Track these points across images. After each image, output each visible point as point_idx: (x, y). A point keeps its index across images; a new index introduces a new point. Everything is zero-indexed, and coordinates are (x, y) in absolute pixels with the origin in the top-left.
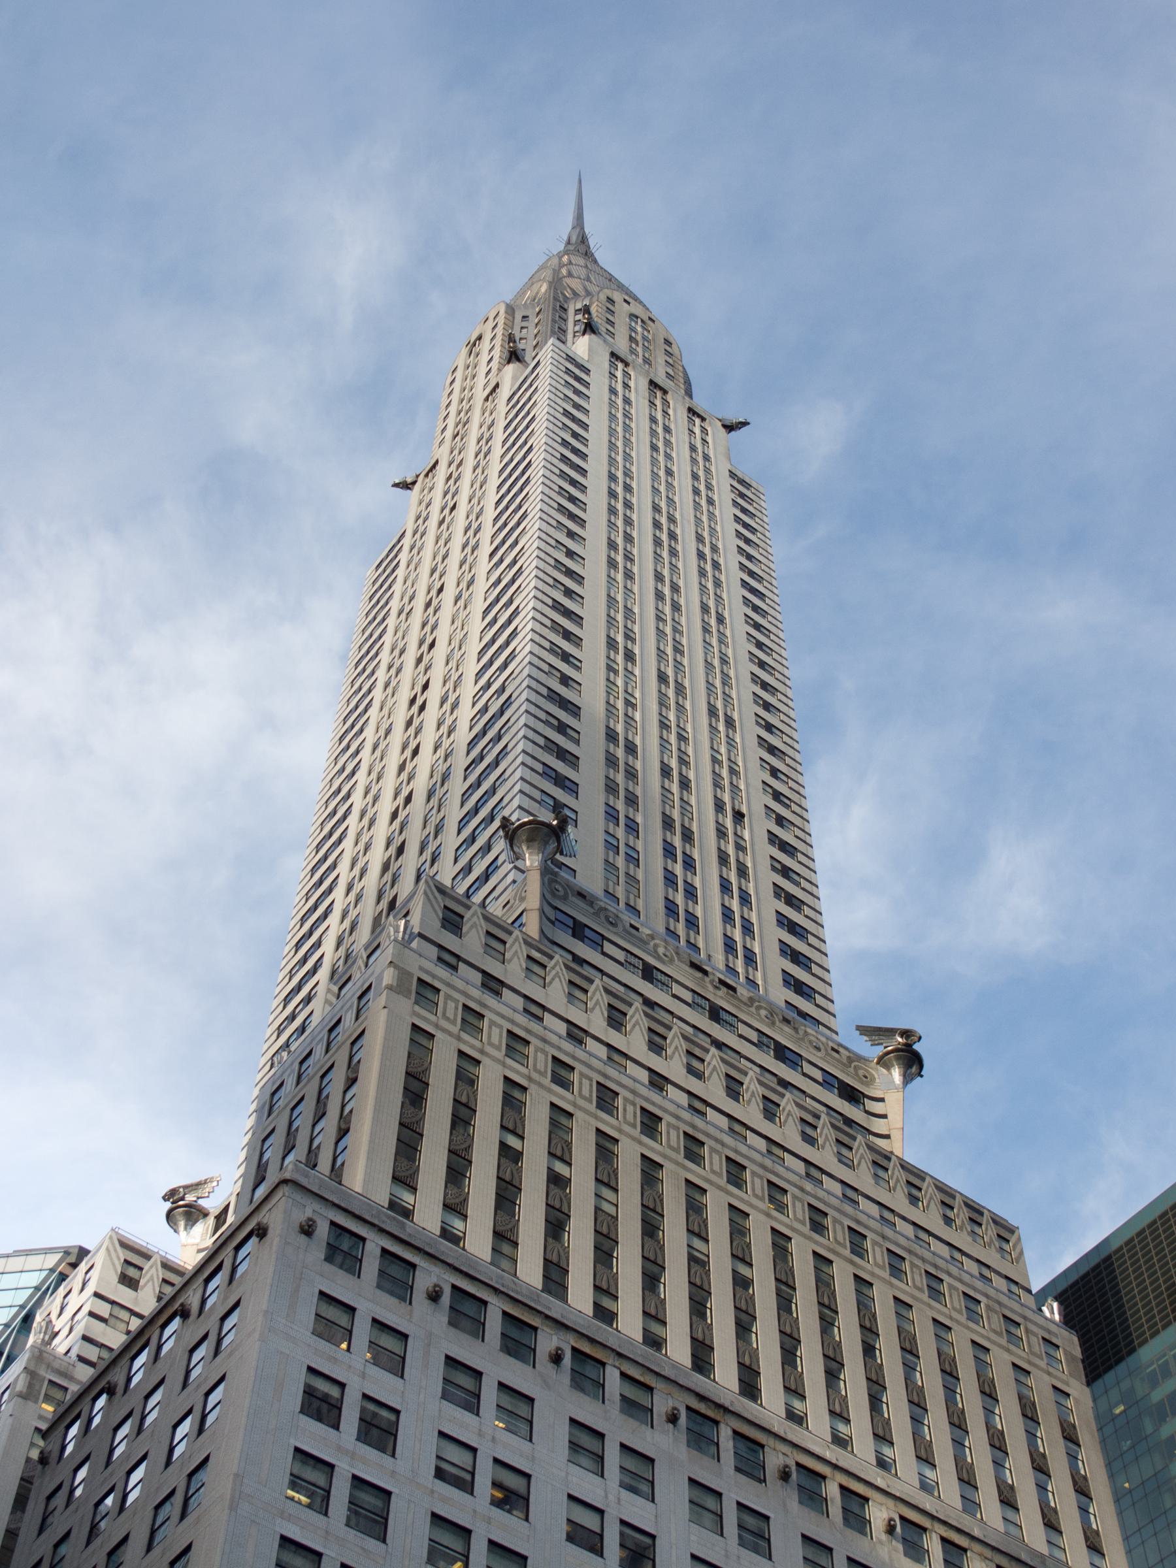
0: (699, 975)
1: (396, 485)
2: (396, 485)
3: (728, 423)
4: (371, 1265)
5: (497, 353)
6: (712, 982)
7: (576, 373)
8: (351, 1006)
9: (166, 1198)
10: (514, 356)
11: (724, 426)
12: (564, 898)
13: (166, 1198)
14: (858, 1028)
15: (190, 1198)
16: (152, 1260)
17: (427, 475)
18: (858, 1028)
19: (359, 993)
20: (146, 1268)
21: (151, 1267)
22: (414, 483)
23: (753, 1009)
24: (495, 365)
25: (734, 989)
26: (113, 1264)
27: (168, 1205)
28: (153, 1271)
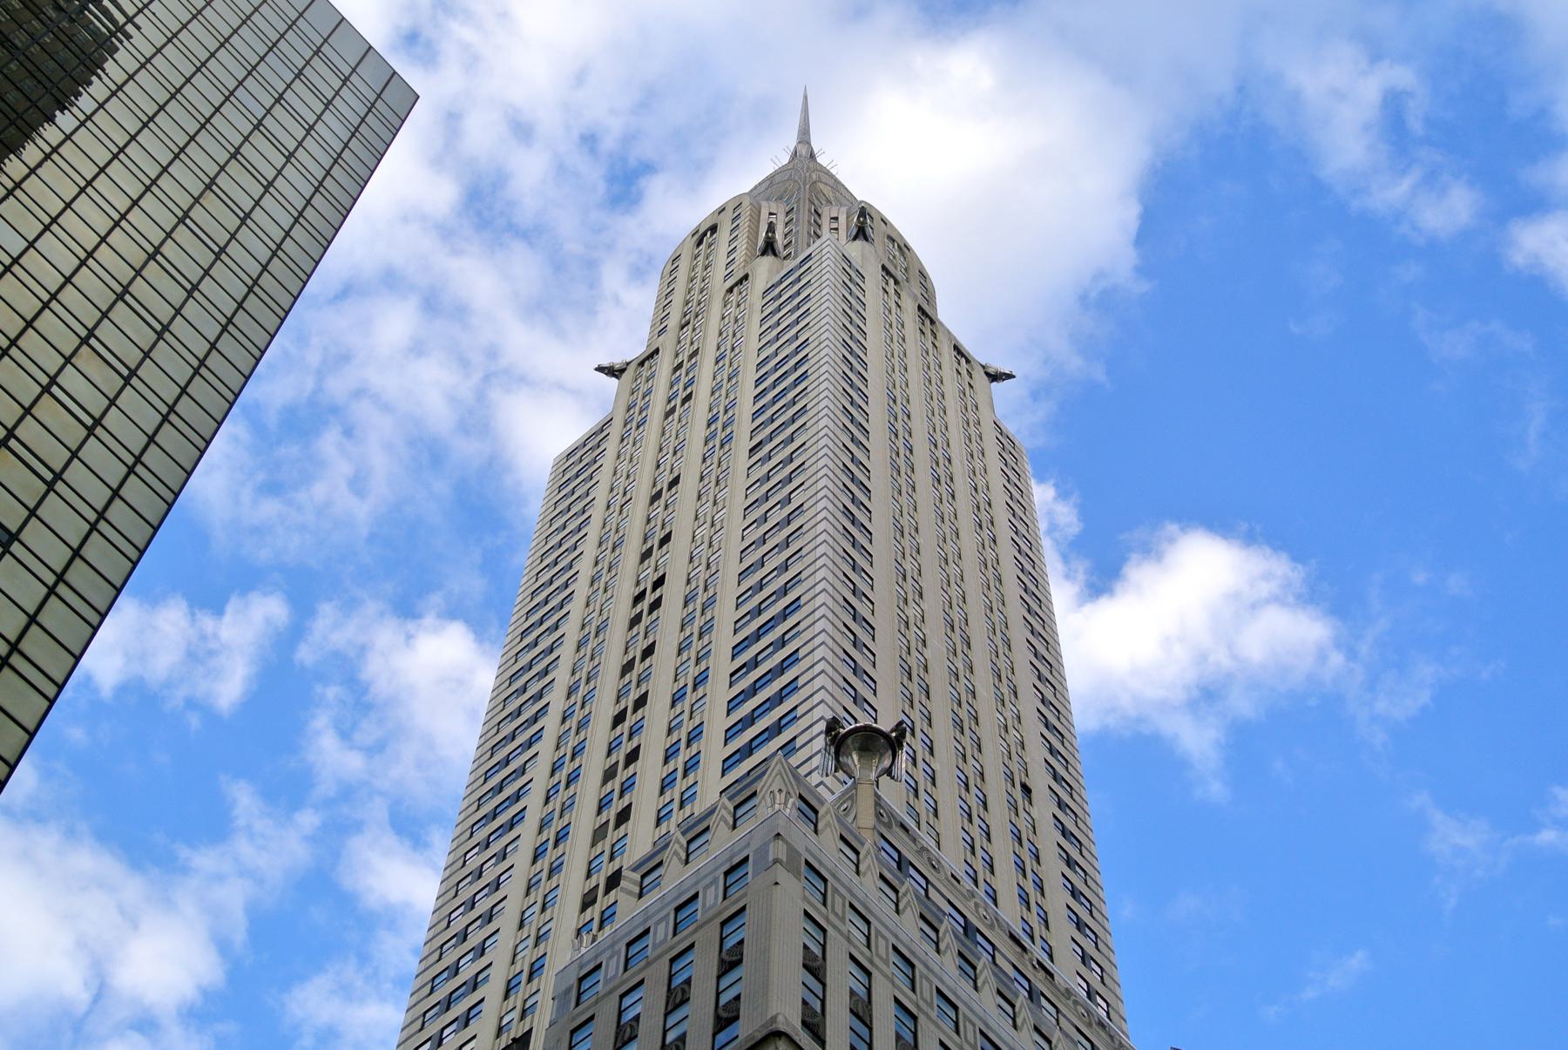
0: (1019, 950)
1: (600, 369)
2: (600, 369)
3: (991, 371)
5: (742, 244)
6: (1031, 961)
7: (852, 275)
8: (714, 882)
10: (769, 248)
11: (987, 374)
12: (889, 826)
17: (642, 364)
19: (727, 867)
22: (622, 371)
24: (740, 255)
25: (1052, 976)
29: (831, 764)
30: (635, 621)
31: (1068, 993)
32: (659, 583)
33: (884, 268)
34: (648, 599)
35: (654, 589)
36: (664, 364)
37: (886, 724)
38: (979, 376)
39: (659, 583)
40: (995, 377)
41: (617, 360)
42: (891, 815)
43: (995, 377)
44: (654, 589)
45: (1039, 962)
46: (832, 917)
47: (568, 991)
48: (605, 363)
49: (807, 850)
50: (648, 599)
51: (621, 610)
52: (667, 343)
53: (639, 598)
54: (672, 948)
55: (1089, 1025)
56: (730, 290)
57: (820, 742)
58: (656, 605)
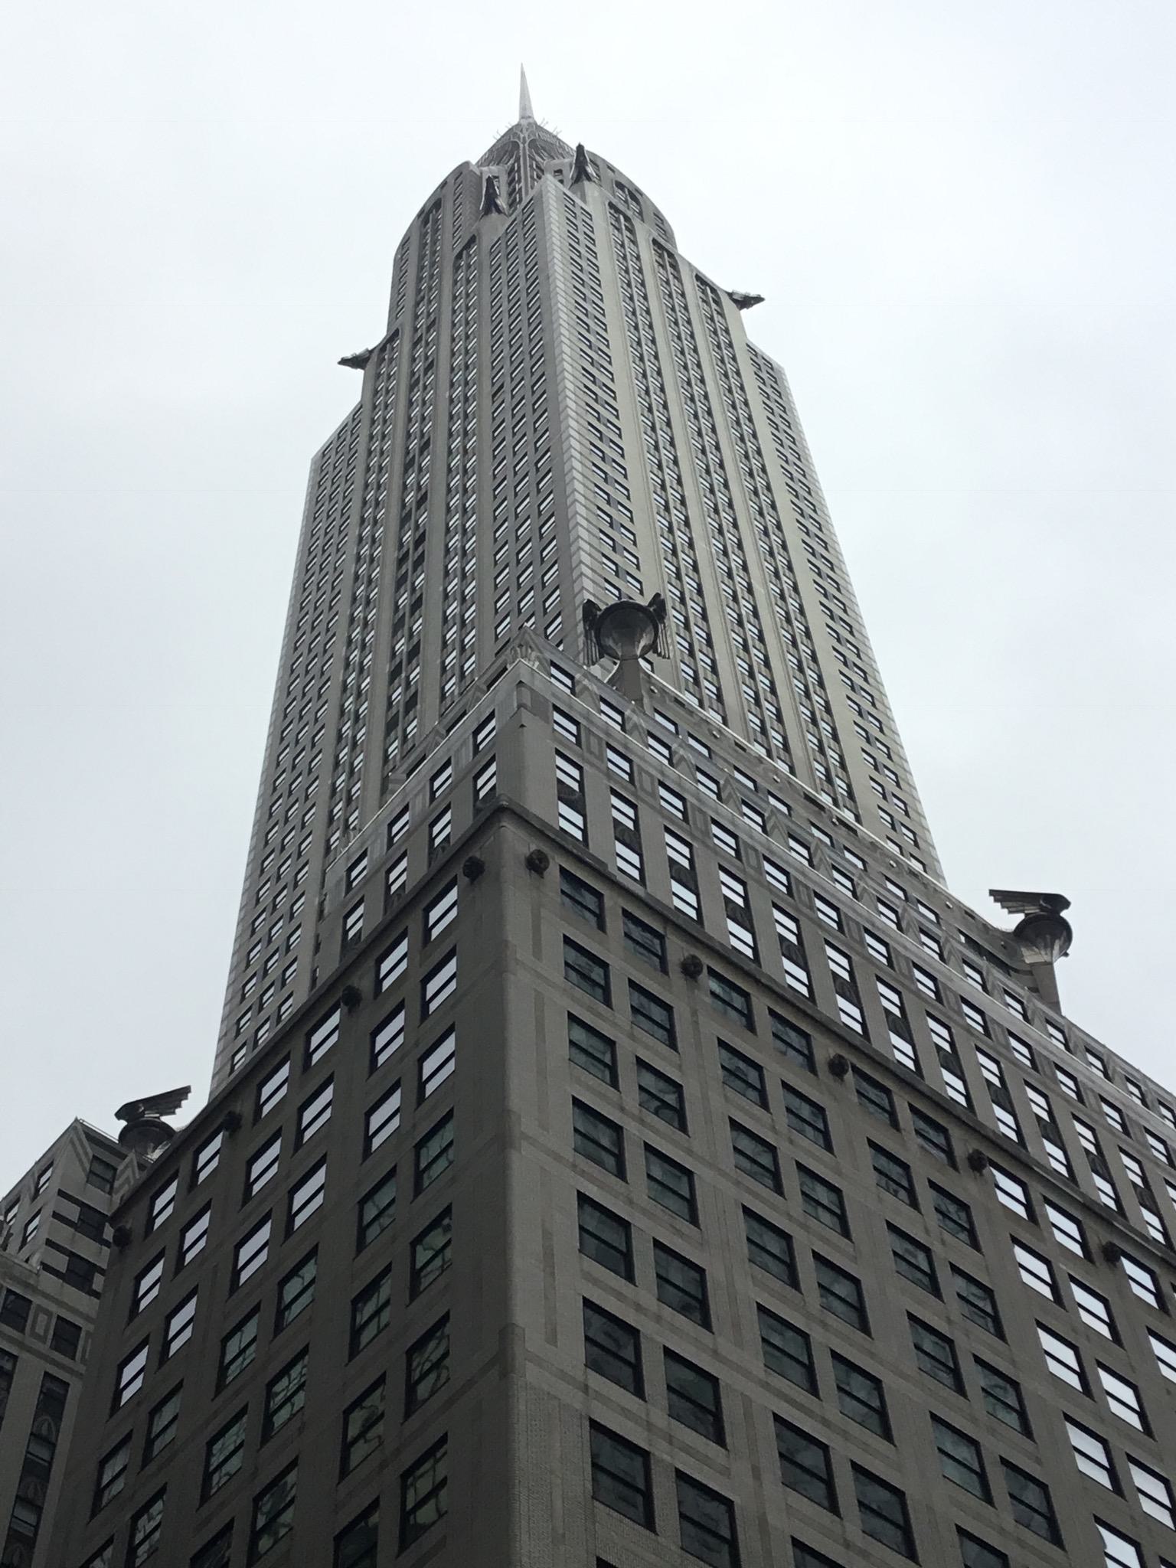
1: (344, 362)
4: (616, 924)
5: (467, 209)
8: (464, 743)
9: (119, 1115)
11: (735, 301)
13: (119, 1115)
14: (993, 893)
15: (150, 1115)
16: (127, 1160)
18: (993, 893)
20: (120, 1168)
21: (126, 1167)
23: (878, 855)
26: (80, 1160)
27: (123, 1123)
28: (129, 1172)
29: (595, 651)
30: (400, 582)
31: (874, 846)
32: (420, 541)
33: (611, 205)
34: (411, 559)
35: (416, 549)
36: (404, 343)
37: (644, 601)
38: (726, 303)
39: (420, 541)
40: (746, 302)
41: (358, 350)
42: (663, 690)
43: (746, 302)
44: (416, 549)
45: (838, 819)
46: (587, 755)
47: (339, 882)
48: (348, 355)
49: (554, 695)
50: (411, 559)
51: (385, 573)
52: (406, 317)
53: (401, 561)
54: (430, 815)
55: (897, 874)
56: (459, 256)
57: (581, 628)
58: (419, 562)
